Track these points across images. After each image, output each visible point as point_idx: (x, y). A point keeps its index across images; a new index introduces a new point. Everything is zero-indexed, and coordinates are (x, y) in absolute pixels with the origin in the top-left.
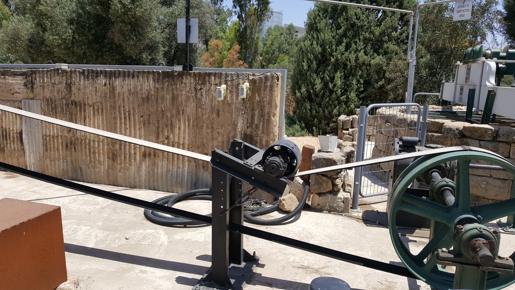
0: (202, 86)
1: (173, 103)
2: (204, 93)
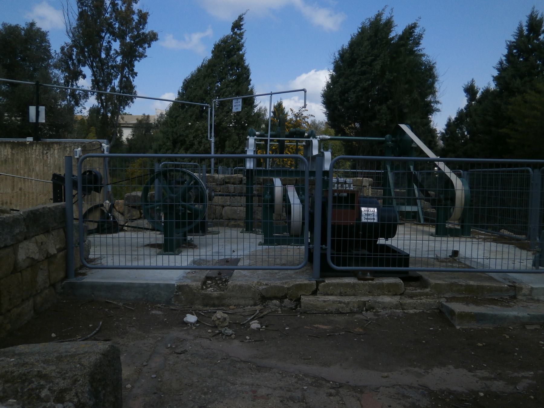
0: (48, 151)
1: (25, 163)
2: (49, 156)
